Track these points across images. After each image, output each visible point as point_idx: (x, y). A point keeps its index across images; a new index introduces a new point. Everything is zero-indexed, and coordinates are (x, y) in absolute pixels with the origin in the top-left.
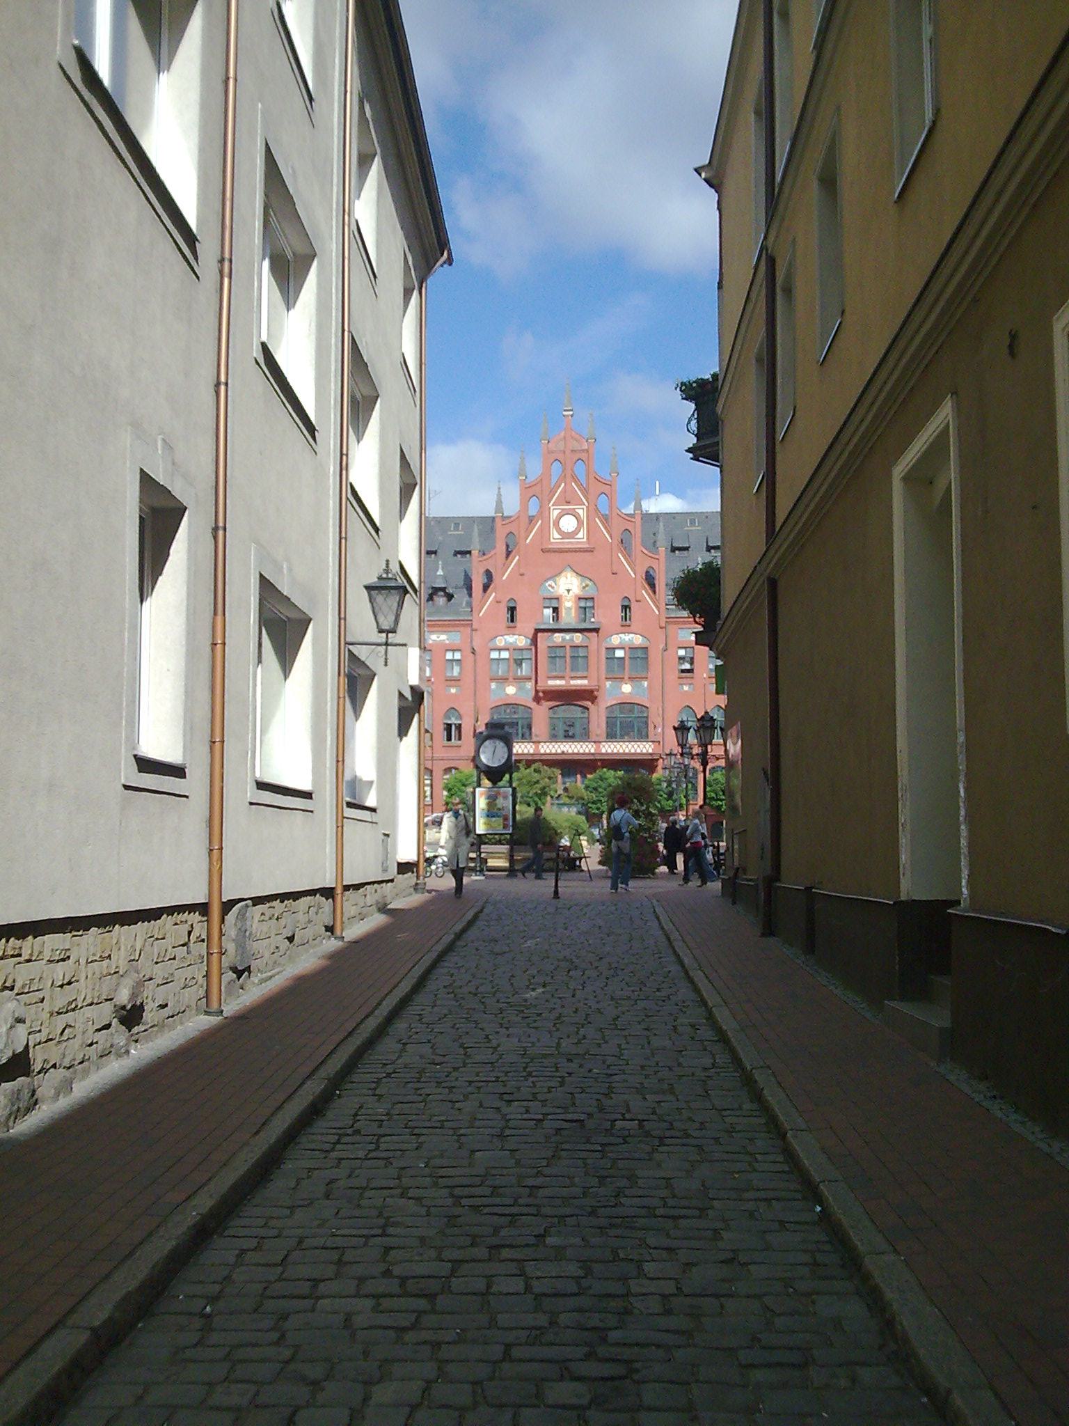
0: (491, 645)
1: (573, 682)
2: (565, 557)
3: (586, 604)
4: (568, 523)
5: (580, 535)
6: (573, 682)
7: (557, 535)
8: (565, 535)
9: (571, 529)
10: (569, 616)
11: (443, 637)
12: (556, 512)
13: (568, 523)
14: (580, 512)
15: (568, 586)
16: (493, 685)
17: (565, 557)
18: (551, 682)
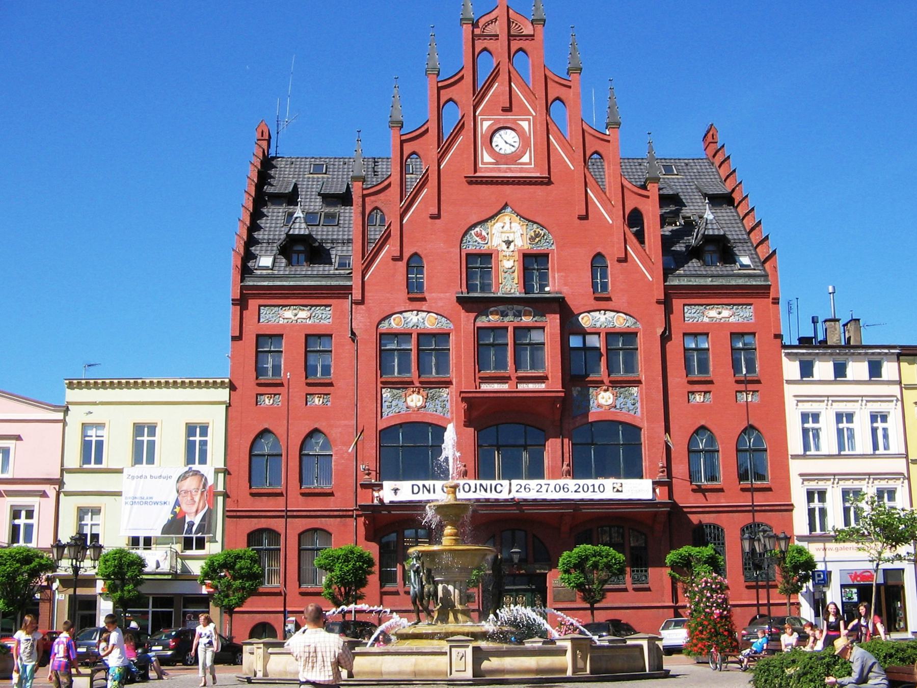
0: (384, 327)
1: (522, 387)
2: (503, 188)
3: (533, 263)
4: (506, 142)
5: (526, 159)
6: (522, 387)
7: (487, 158)
8: (501, 159)
9: (509, 150)
10: (508, 283)
11: (303, 314)
12: (486, 124)
13: (506, 142)
14: (525, 125)
15: (508, 236)
16: (387, 394)
17: (503, 188)
18: (485, 387)
